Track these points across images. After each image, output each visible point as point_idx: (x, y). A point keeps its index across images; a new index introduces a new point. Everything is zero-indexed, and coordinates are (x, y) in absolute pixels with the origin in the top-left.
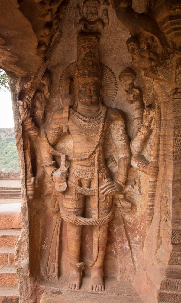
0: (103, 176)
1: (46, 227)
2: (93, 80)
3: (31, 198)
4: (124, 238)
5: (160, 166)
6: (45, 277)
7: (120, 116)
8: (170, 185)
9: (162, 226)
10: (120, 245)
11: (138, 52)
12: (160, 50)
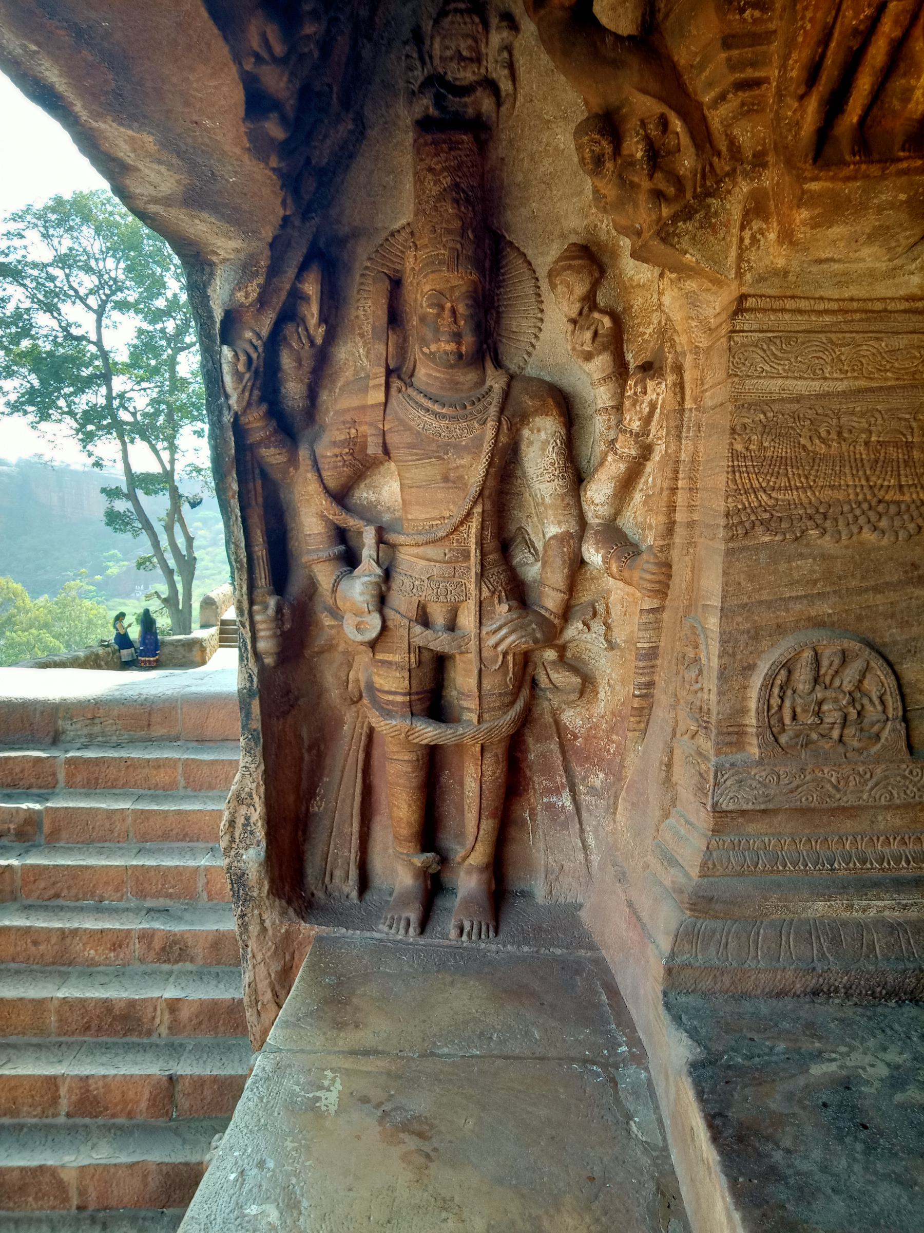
0: (493, 593)
1: (322, 747)
3: (269, 661)
4: (558, 778)
6: (320, 894)
8: (713, 622)
10: (545, 800)
12: (687, 163)
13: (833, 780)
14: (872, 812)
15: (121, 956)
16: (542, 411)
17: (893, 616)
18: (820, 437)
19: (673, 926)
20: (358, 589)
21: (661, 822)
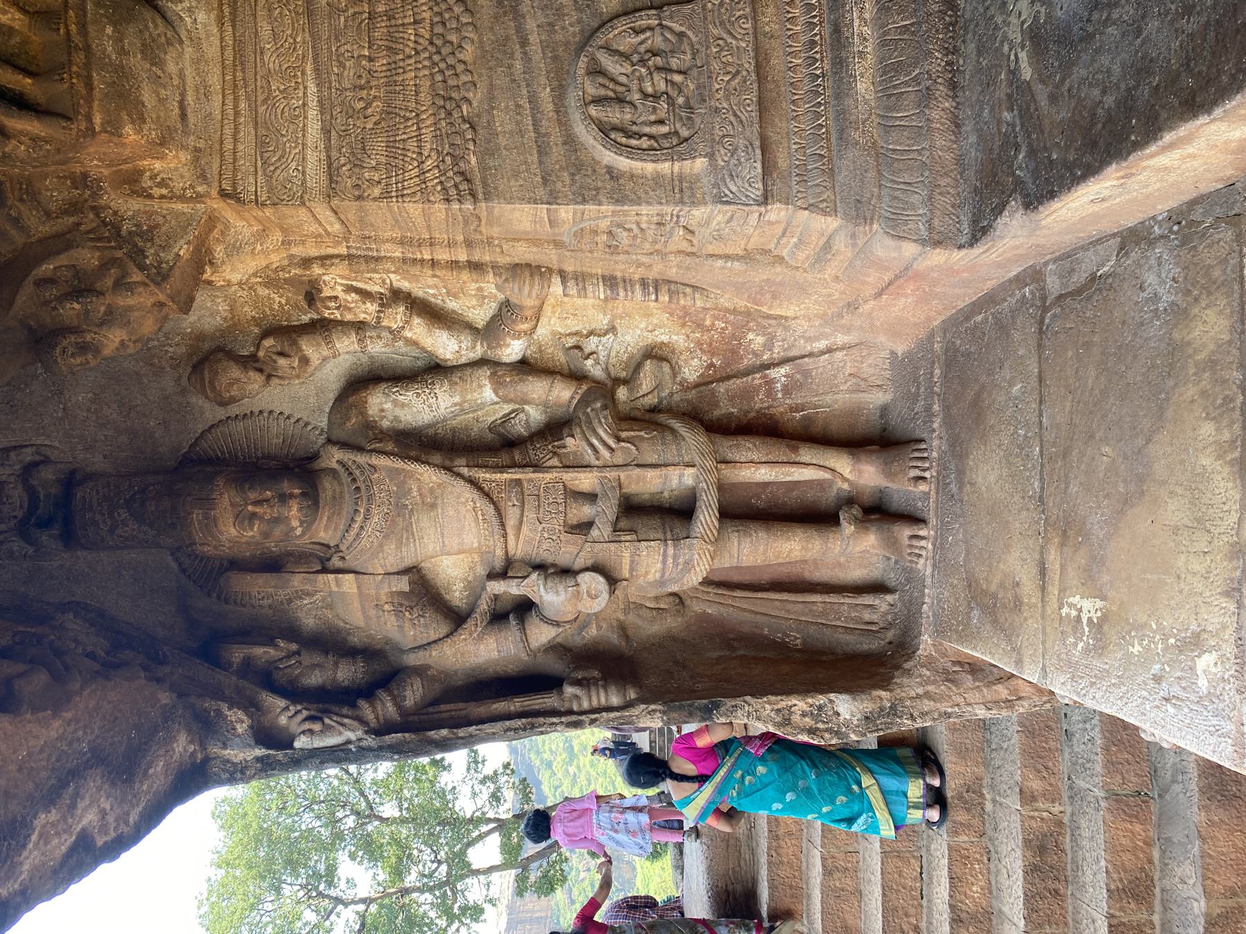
0: (555, 453)
1: (731, 636)
2: (222, 493)
3: (632, 694)
5: (508, 260)
6: (890, 635)
7: (351, 400)
8: (565, 213)
9: (711, 249)
10: (780, 395)
11: (90, 331)
13: (726, 79)
14: (761, 38)
15: (978, 856)
16: (362, 409)
17: (551, 25)
18: (365, 108)
19: (890, 242)
20: (552, 597)
21: (788, 266)
